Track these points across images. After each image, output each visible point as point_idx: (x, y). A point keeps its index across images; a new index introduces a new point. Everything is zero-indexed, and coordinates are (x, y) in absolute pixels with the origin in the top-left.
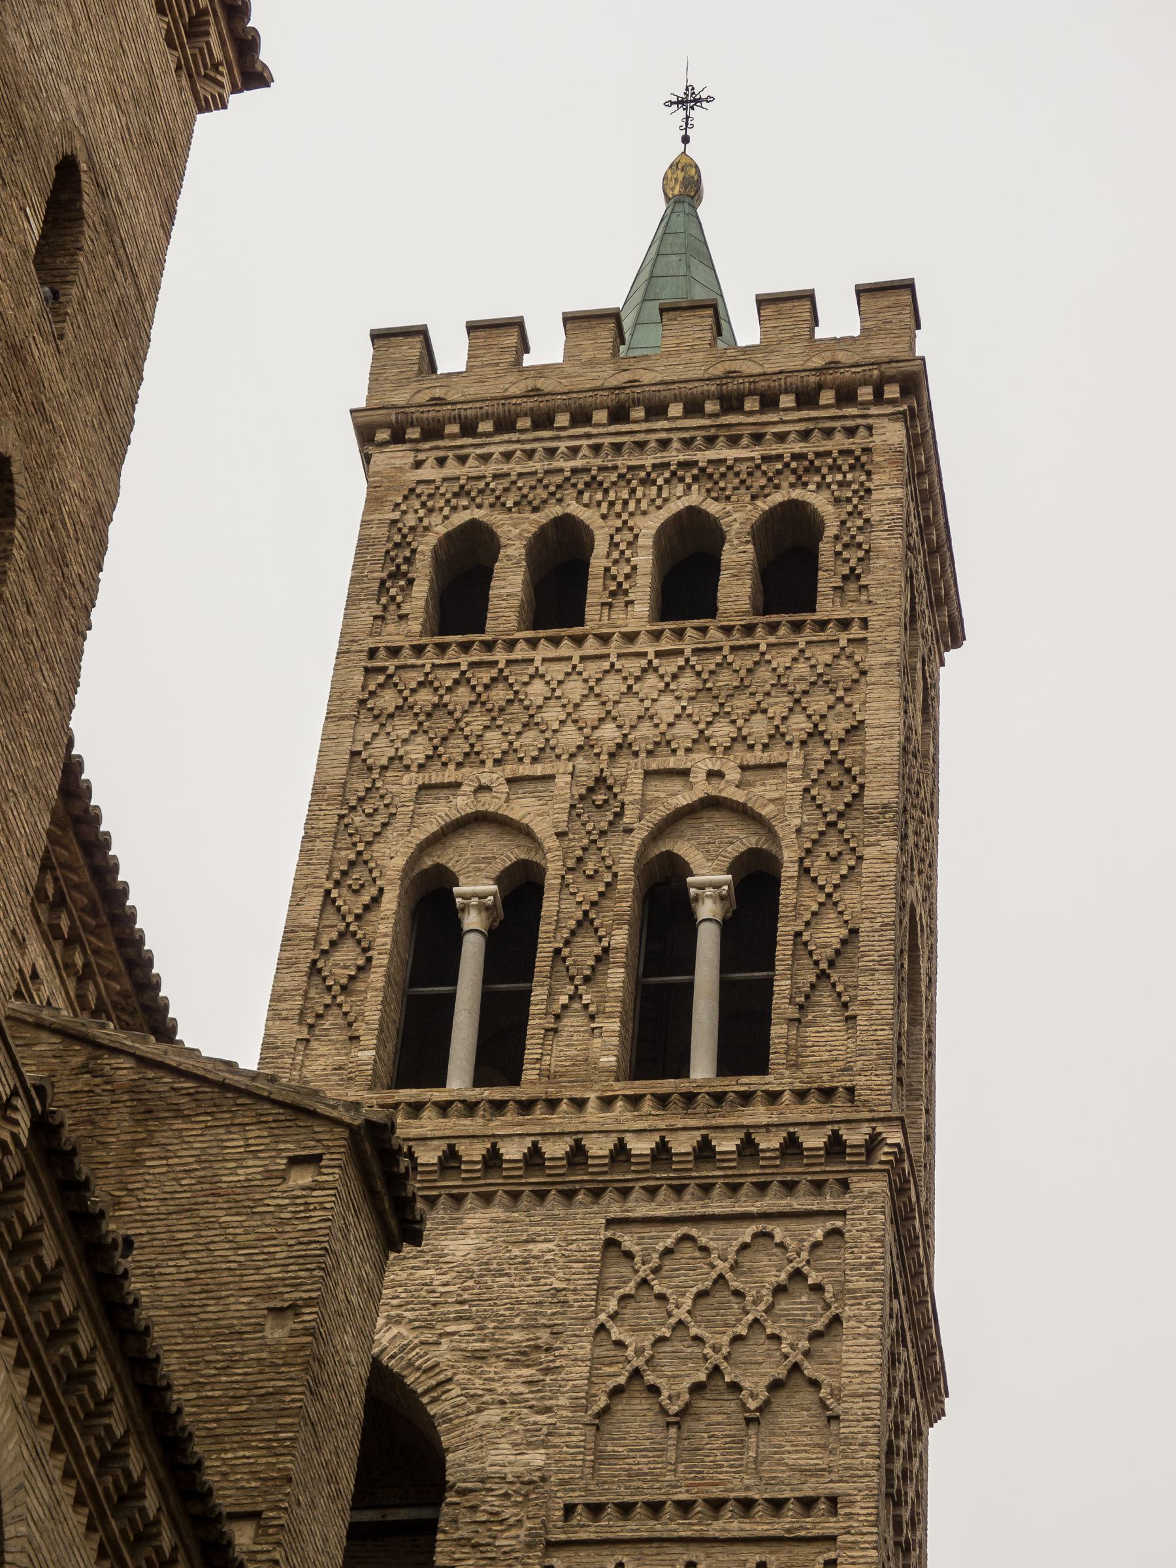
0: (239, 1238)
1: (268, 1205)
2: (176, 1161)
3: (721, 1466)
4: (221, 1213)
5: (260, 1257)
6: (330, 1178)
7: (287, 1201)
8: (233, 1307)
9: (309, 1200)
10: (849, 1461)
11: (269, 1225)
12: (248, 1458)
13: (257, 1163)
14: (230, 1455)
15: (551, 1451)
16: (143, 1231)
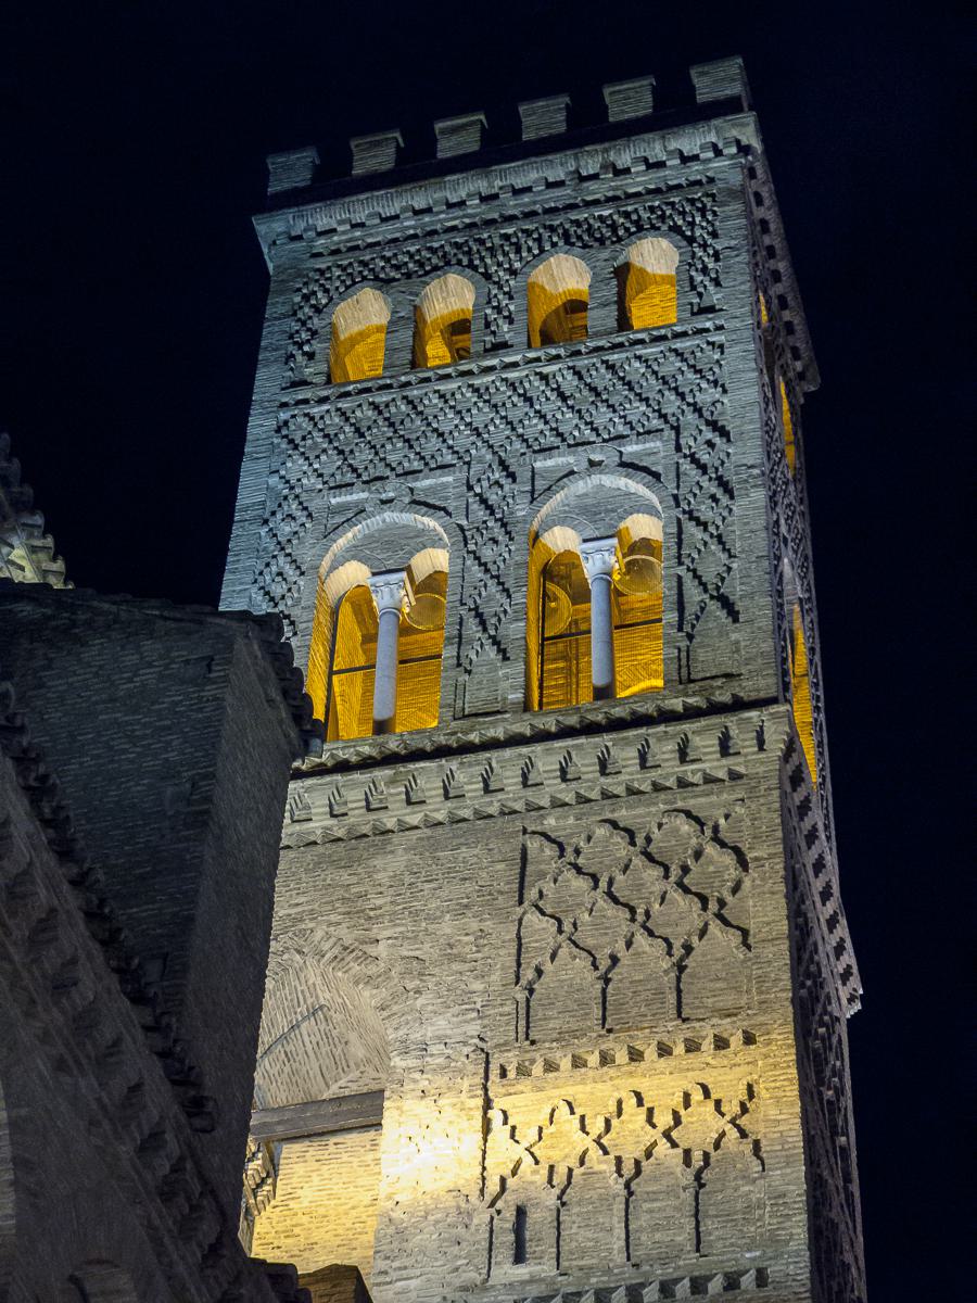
0: (137, 733)
1: (163, 703)
2: (75, 678)
3: (646, 1016)
4: (119, 715)
5: (157, 746)
6: (222, 674)
7: (180, 698)
8: (134, 789)
9: (202, 694)
10: (763, 997)
11: (167, 718)
12: (153, 909)
13: (152, 670)
14: (135, 910)
15: (486, 1022)
16: (47, 738)
